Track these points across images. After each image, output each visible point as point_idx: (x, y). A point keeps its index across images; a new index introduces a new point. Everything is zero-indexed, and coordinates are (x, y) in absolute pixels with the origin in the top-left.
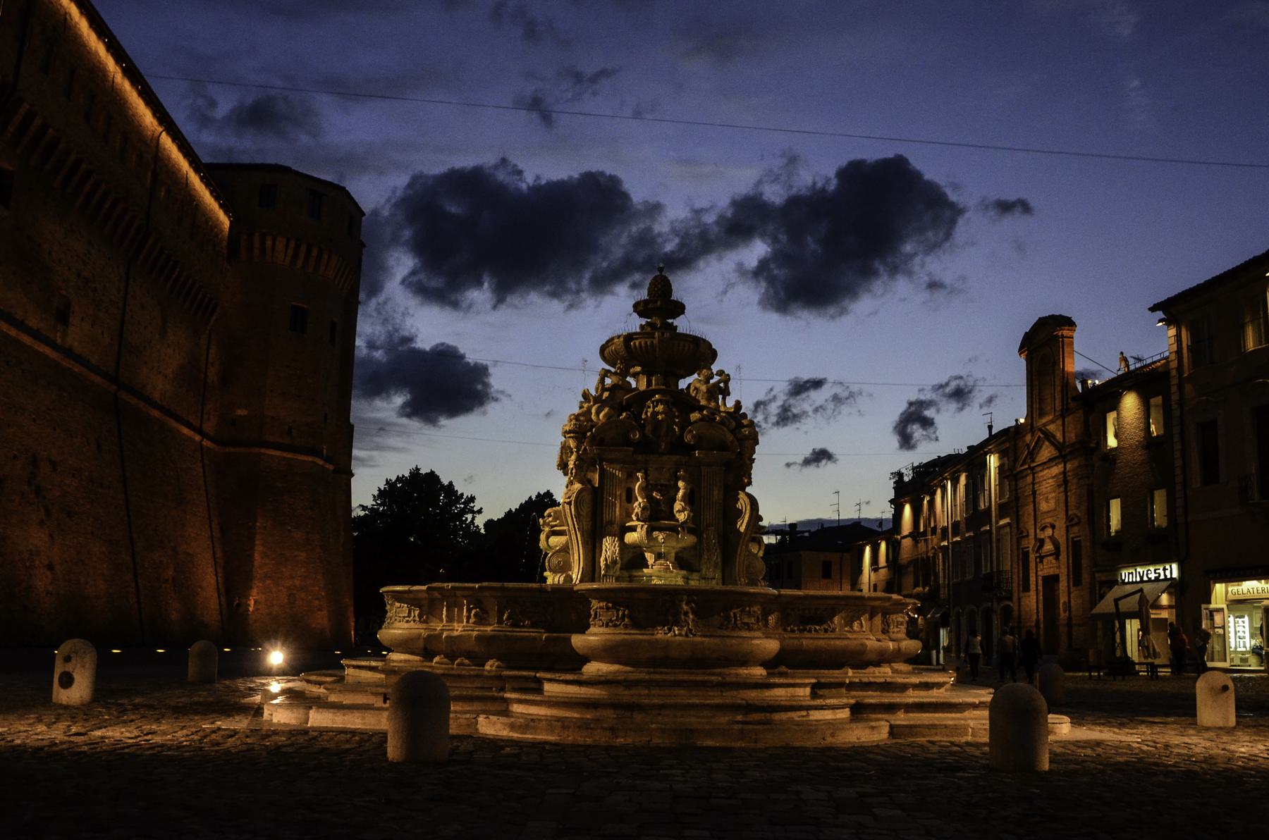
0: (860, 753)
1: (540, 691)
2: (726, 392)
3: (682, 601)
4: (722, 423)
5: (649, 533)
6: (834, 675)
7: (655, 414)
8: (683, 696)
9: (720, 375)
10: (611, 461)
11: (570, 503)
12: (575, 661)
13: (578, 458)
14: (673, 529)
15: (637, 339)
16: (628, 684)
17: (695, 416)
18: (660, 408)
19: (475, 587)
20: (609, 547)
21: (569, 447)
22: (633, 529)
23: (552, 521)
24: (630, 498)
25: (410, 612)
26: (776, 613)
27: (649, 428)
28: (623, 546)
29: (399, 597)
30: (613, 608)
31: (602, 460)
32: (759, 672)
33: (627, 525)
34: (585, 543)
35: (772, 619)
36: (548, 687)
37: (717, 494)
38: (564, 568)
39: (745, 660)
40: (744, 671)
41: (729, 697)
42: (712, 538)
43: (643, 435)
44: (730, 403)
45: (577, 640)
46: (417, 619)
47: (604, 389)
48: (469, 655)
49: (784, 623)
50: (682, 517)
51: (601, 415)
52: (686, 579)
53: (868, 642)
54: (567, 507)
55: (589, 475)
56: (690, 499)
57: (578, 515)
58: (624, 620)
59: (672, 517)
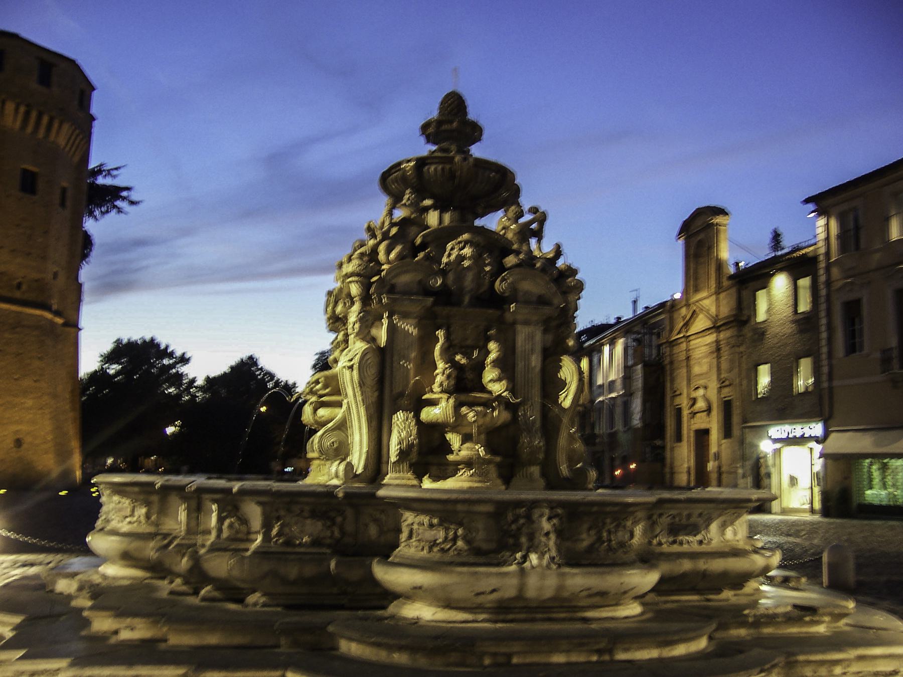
2: (538, 234)
3: (542, 516)
7: (461, 258)
9: (535, 213)
10: (405, 316)
11: (351, 367)
14: (487, 404)
15: (431, 164)
17: (510, 260)
18: (467, 251)
19: (229, 491)
21: (349, 295)
22: (433, 403)
23: (321, 389)
25: (133, 511)
26: (643, 524)
29: (119, 489)
30: (440, 524)
33: (423, 398)
37: (536, 361)
38: (340, 452)
44: (547, 247)
46: (142, 519)
47: (392, 225)
51: (392, 256)
54: (347, 373)
55: (374, 332)
57: (362, 384)
58: (455, 544)
59: (483, 389)
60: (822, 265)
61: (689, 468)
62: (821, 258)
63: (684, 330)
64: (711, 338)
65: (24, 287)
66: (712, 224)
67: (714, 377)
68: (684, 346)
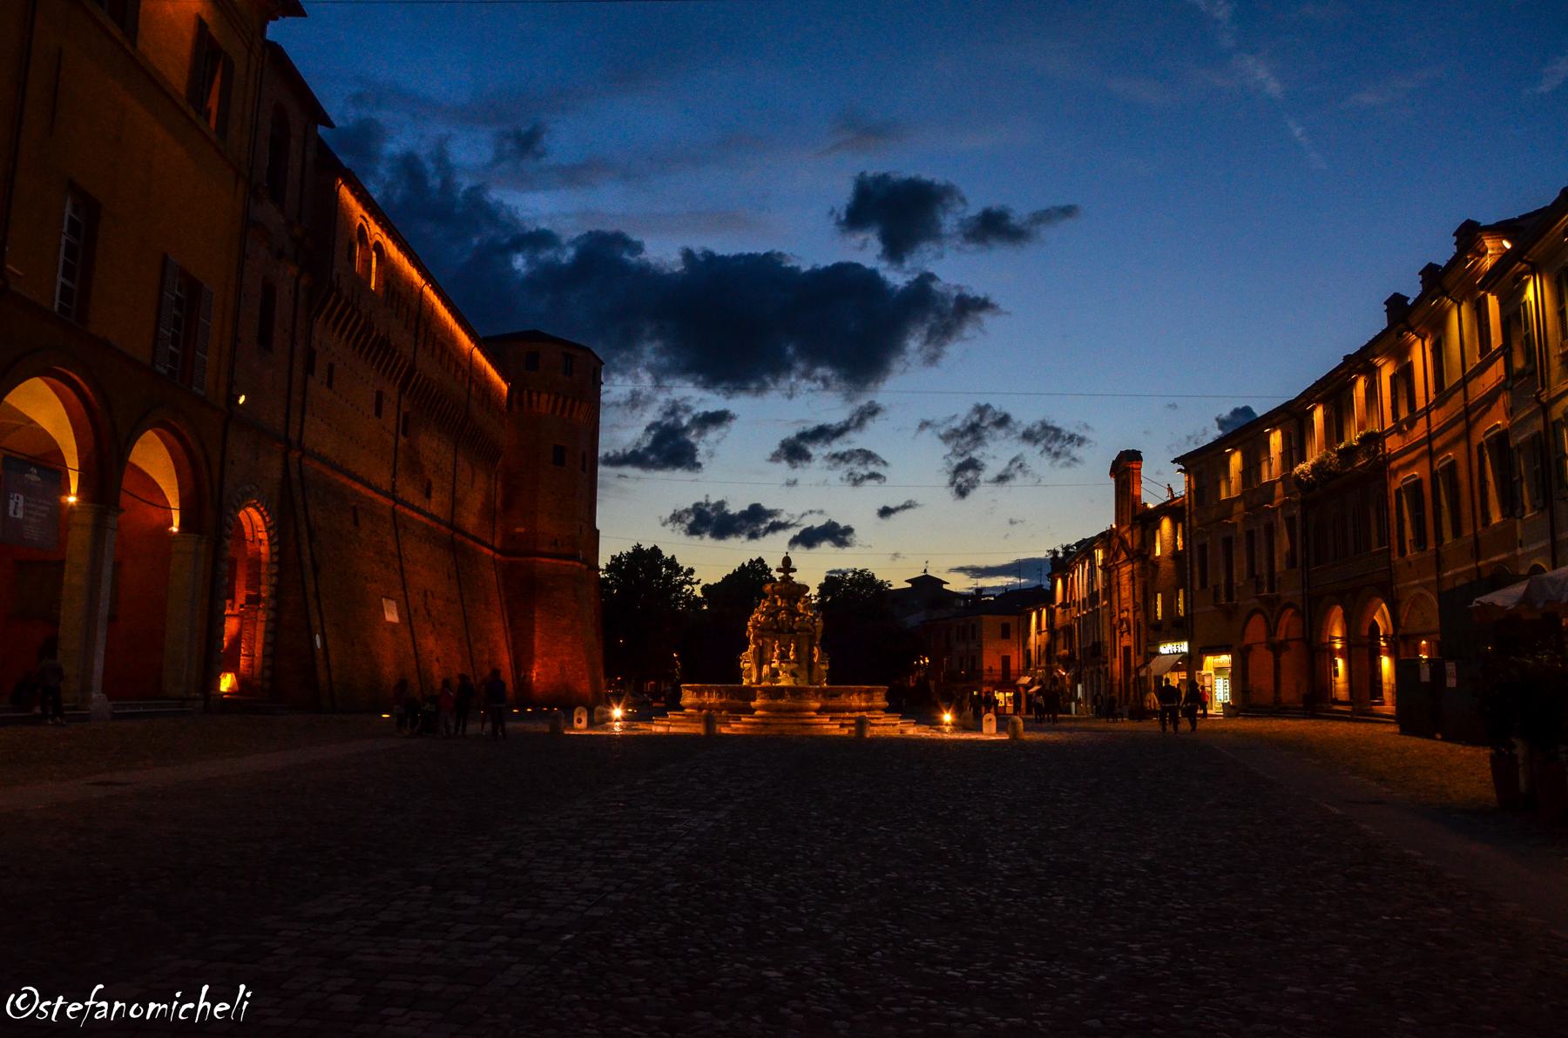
0: (843, 737)
1: (740, 720)
4: (807, 621)
5: (780, 663)
6: (838, 715)
8: (786, 721)
10: (766, 636)
12: (751, 711)
13: (754, 636)
14: (789, 663)
16: (767, 717)
17: (797, 619)
20: (766, 669)
22: (774, 662)
24: (774, 650)
27: (780, 624)
28: (771, 668)
29: (688, 688)
31: (762, 636)
32: (813, 714)
34: (757, 668)
35: (820, 696)
36: (743, 719)
37: (806, 648)
38: (749, 676)
39: (807, 710)
40: (808, 713)
41: (800, 721)
42: (805, 665)
43: (778, 626)
45: (752, 704)
48: (717, 709)
49: (824, 696)
50: (792, 658)
52: (795, 682)
53: (853, 704)
56: (796, 650)
59: (789, 658)
60: (1187, 513)
61: (1120, 680)
62: (1187, 508)
63: (1114, 559)
64: (1129, 568)
65: (559, 543)
66: (1129, 468)
67: (1132, 602)
68: (1116, 572)
